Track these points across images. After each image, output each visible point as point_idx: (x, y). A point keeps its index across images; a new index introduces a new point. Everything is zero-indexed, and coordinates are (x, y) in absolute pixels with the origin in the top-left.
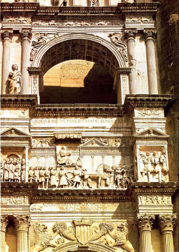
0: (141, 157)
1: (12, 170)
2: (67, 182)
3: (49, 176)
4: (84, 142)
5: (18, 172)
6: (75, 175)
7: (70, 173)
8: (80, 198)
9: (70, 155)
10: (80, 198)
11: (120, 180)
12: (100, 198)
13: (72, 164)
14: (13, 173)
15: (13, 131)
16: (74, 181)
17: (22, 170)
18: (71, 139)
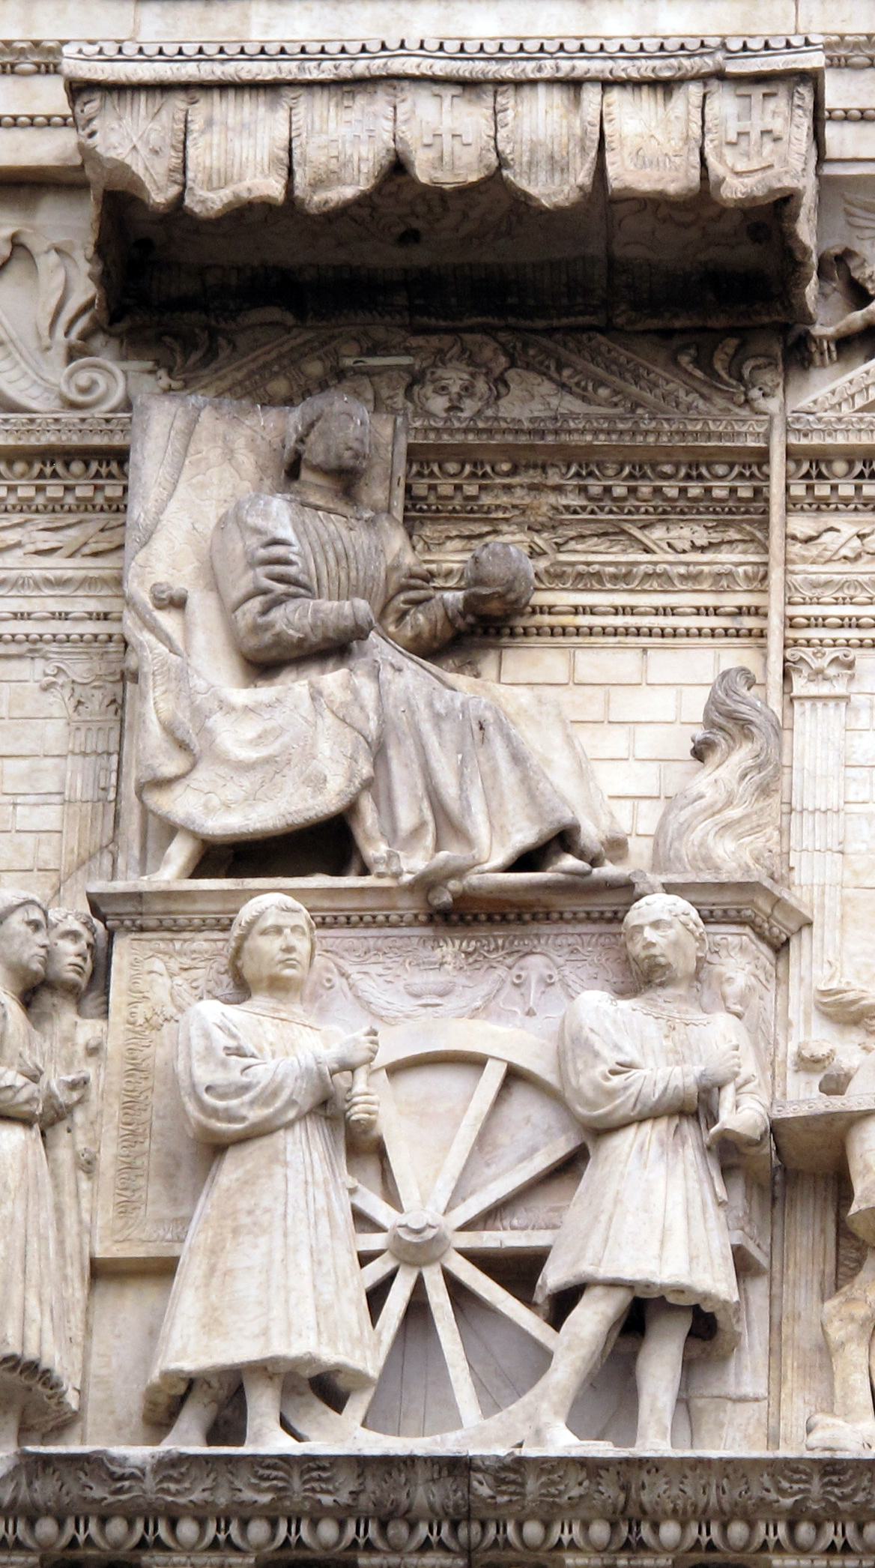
2: (377, 1297)
6: (602, 1130)
7: (476, 1062)
13: (525, 836)
16: (553, 1277)
18: (522, 202)
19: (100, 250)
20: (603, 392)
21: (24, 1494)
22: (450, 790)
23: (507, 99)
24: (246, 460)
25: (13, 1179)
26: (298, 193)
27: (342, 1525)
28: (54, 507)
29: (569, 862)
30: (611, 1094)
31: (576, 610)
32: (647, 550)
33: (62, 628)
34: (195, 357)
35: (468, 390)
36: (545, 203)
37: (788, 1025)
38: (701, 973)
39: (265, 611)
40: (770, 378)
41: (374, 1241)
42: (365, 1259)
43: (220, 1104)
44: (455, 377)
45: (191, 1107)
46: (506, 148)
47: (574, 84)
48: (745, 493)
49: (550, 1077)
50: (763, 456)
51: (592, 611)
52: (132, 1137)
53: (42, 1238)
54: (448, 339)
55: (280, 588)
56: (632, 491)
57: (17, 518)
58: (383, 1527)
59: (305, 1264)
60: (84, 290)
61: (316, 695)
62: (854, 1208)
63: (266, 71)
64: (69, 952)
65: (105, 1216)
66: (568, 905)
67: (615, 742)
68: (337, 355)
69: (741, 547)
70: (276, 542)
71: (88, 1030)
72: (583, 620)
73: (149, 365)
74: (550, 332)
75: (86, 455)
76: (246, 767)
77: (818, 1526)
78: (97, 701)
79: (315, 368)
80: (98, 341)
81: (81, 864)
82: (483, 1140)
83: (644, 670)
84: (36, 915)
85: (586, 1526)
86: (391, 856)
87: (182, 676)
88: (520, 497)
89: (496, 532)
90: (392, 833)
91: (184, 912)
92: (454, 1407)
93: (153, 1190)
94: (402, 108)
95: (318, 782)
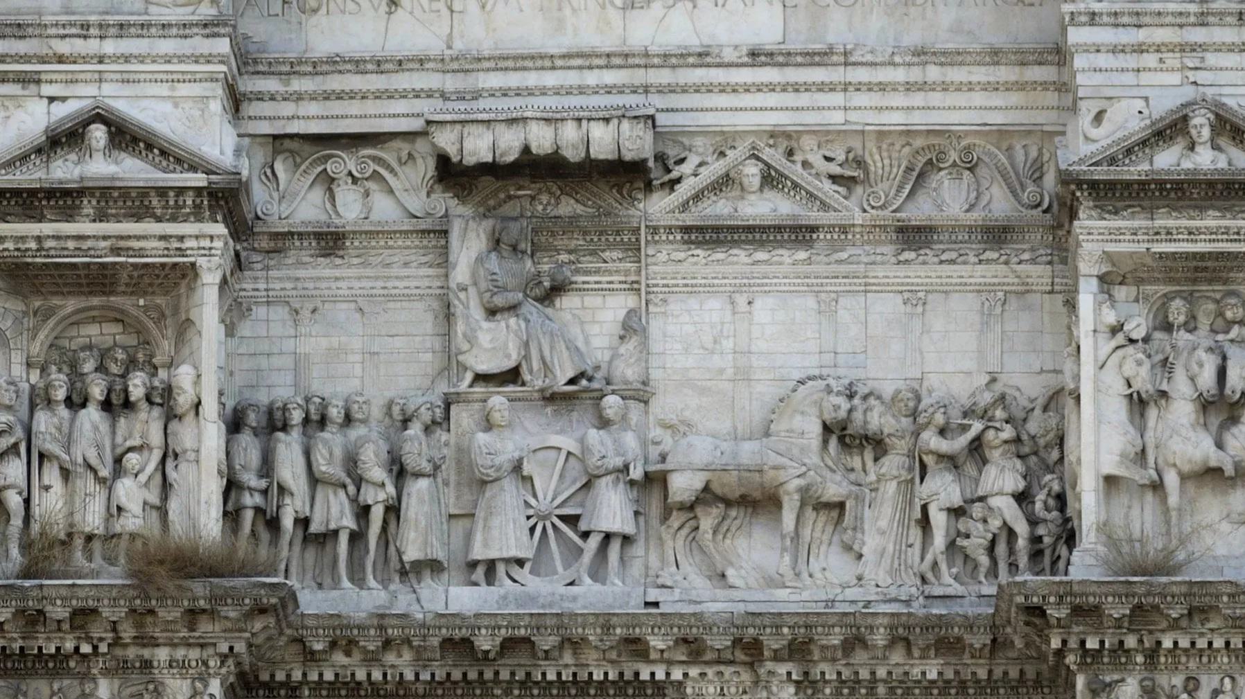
0: (1113, 344)
1: (94, 461)
3: (391, 489)
4: (678, 180)
5: (143, 478)
7: (560, 449)
8: (628, 676)
9: (557, 289)
10: (628, 676)
11: (957, 512)
12: (782, 669)
13: (570, 374)
14: (101, 481)
15: (98, 134)
16: (583, 526)
17: (169, 455)
19: (436, 168)
20: (590, 203)
21: (437, 624)
22: (548, 359)
23: (559, 125)
24: (483, 236)
25: (426, 498)
26: (497, 160)
27: (526, 629)
28: (426, 247)
29: (584, 382)
30: (598, 467)
31: (584, 283)
32: (605, 262)
33: (430, 291)
34: (466, 193)
35: (549, 203)
36: (571, 160)
37: (649, 429)
38: (624, 418)
39: (491, 297)
40: (640, 196)
41: (531, 512)
42: (529, 518)
43: (485, 471)
44: (544, 198)
45: (476, 471)
46: (559, 143)
47: (579, 120)
48: (634, 240)
49: (580, 456)
50: (639, 229)
51: (588, 283)
52: (459, 473)
53: (435, 516)
54: (542, 185)
55: (496, 290)
56: (600, 239)
57: (414, 251)
58: (538, 629)
59: (512, 525)
60: (430, 174)
61: (508, 327)
62: (669, 500)
63: (485, 116)
64: (439, 412)
65: (452, 500)
66: (584, 395)
67: (595, 329)
68: (508, 191)
69: (632, 259)
70: (494, 274)
71: (444, 437)
72: (586, 286)
73: (451, 195)
74: (572, 182)
75: (434, 232)
76: (486, 350)
77: (660, 628)
78: (441, 317)
79: (502, 196)
80: (436, 187)
81: (439, 374)
82: (561, 476)
83: (604, 302)
84: (429, 406)
85: (595, 628)
86: (532, 380)
87: (467, 317)
88: (566, 242)
89: (559, 254)
90: (531, 372)
91: (470, 397)
92: (555, 567)
93: (466, 490)
94: (528, 128)
95: (508, 356)
